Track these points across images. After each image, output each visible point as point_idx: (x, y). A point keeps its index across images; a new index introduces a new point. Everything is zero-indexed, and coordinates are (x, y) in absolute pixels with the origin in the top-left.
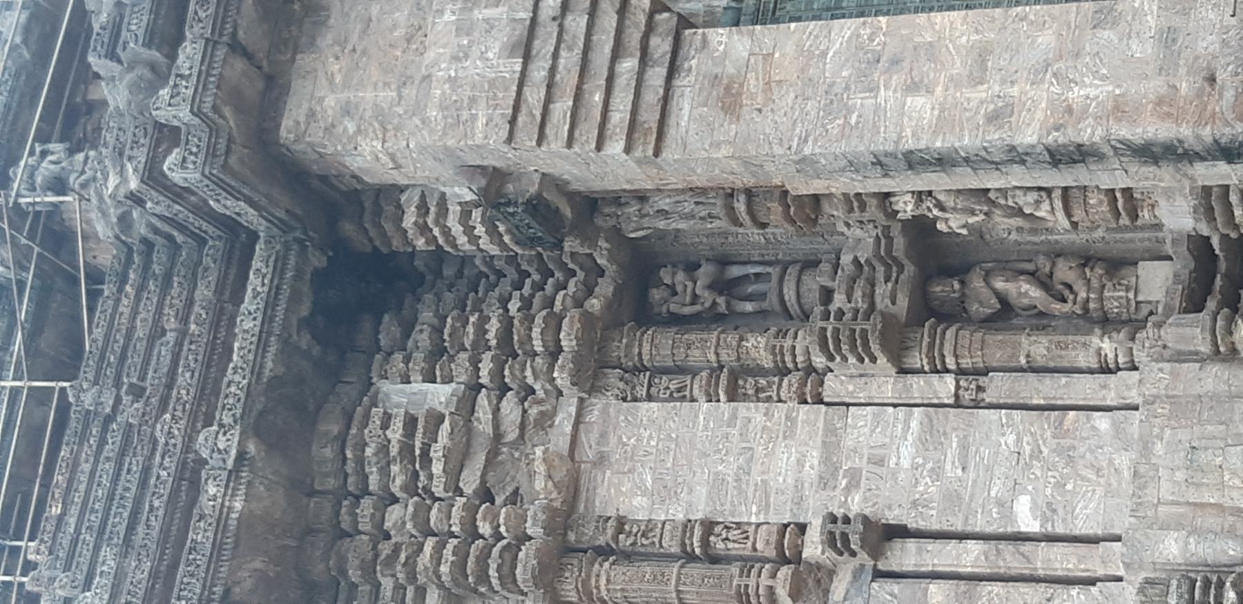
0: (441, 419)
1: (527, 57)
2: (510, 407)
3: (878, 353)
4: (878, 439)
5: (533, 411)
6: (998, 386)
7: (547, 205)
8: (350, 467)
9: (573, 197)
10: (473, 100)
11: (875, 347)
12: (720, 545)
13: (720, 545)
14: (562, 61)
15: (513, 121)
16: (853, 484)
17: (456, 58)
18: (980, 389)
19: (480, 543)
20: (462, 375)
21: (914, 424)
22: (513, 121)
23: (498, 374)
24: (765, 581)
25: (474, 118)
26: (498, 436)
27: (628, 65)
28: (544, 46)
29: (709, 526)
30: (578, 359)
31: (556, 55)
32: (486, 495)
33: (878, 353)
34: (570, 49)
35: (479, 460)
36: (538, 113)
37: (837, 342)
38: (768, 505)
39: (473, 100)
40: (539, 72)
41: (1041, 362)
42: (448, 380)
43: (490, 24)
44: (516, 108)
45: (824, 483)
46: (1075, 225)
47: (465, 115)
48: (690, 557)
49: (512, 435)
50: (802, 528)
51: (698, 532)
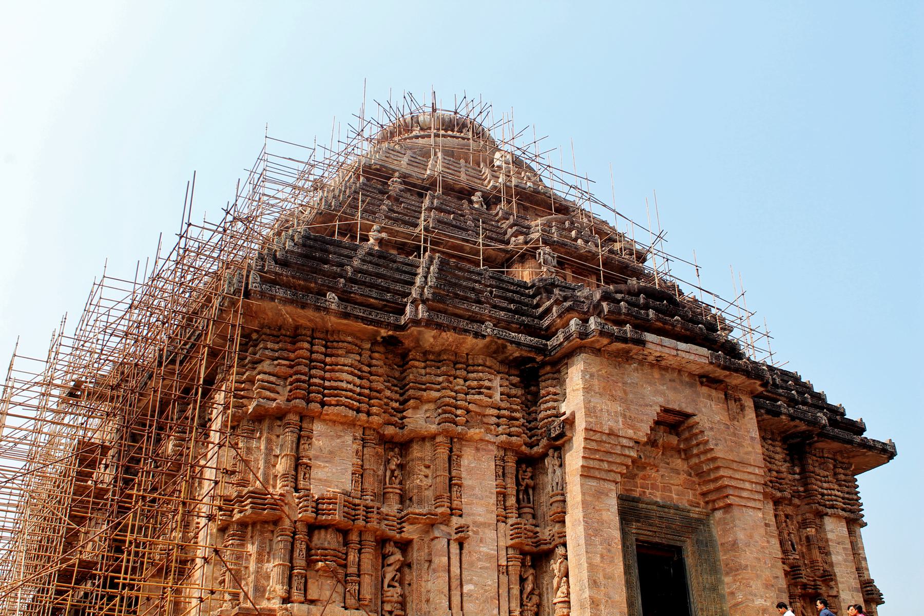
0: (490, 397)
1: (609, 434)
2: (494, 420)
3: (514, 541)
4: (488, 540)
5: (492, 427)
6: (504, 578)
7: (562, 438)
8: (476, 368)
9: (563, 445)
10: (597, 417)
11: (517, 540)
12: (455, 489)
13: (455, 489)
18: (503, 573)
20: (503, 405)
21: (492, 552)
23: (503, 416)
24: (446, 504)
26: (484, 416)
27: (605, 466)
28: (612, 440)
29: (460, 486)
30: (510, 443)
31: (609, 443)
33: (514, 541)
34: (611, 448)
37: (518, 528)
38: (466, 504)
39: (597, 417)
40: (604, 438)
41: (511, 592)
44: (594, 431)
45: (474, 523)
46: (555, 604)
48: (451, 479)
49: (485, 420)
50: (461, 516)
51: (459, 482)
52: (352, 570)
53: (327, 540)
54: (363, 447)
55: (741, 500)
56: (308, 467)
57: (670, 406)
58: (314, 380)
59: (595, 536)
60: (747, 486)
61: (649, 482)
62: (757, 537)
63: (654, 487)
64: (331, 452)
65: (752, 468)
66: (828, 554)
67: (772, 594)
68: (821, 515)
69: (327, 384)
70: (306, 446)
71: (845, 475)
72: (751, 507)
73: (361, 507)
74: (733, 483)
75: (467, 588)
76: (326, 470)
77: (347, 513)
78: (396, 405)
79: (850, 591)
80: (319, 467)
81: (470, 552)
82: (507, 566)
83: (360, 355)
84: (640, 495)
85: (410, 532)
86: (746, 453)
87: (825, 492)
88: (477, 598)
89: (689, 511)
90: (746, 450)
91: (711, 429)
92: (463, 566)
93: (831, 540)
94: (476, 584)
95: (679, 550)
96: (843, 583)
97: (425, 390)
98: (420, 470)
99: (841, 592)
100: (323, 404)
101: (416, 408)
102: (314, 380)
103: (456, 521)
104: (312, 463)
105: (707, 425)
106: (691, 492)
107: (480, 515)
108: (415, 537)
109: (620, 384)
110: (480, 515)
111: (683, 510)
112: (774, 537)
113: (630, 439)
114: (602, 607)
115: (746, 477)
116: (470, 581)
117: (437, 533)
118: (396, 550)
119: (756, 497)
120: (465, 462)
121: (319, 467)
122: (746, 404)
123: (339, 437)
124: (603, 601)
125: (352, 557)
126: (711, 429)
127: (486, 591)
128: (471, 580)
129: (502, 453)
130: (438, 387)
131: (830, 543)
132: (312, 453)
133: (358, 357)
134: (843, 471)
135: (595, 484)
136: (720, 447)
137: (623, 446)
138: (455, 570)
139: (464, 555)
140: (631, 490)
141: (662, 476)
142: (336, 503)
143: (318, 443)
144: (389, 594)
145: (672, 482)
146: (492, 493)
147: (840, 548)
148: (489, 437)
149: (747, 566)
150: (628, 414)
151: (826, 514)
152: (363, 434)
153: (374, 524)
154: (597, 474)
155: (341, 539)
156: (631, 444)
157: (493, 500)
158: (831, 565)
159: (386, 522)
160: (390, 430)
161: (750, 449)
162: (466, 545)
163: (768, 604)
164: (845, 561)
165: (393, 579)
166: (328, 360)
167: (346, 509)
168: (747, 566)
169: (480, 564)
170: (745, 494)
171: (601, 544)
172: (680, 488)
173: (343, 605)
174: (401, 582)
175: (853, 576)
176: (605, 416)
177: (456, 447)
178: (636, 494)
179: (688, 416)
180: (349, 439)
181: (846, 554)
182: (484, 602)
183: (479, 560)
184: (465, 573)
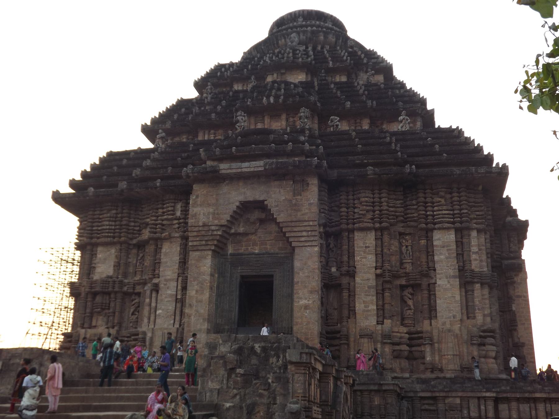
2: (177, 226)
10: (196, 218)
14: (203, 232)
15: (192, 226)
16: (165, 285)
17: (204, 213)
19: (155, 226)
22: (192, 226)
25: (193, 219)
27: (204, 242)
28: (206, 228)
29: (159, 263)
32: (163, 225)
35: (168, 223)
36: (194, 230)
40: (200, 229)
42: (181, 214)
43: (209, 218)
44: (194, 226)
45: (166, 280)
47: (194, 218)
50: (159, 277)
52: (111, 310)
53: (98, 299)
54: (121, 253)
55: (301, 243)
56: (94, 268)
57: (248, 200)
58: (94, 228)
59: (194, 281)
60: (304, 234)
61: (251, 242)
62: (310, 263)
63: (255, 244)
64: (105, 259)
65: (308, 222)
66: (433, 255)
67: (314, 296)
68: (432, 230)
69: (99, 228)
70: (94, 259)
71: (460, 197)
72: (309, 246)
73: (111, 283)
74: (292, 234)
75: (159, 312)
76: (102, 267)
77: (103, 286)
78: (138, 228)
79: (447, 278)
80: (99, 267)
81: (161, 295)
82: (182, 298)
83: (117, 210)
84: (244, 251)
85: (138, 289)
86: (303, 215)
87: (435, 213)
88: (163, 317)
89: (277, 254)
90: (303, 212)
91: (277, 206)
92: (158, 302)
93: (437, 246)
94: (163, 310)
95: (272, 276)
96: (442, 273)
97: (144, 219)
98: (147, 258)
99: (437, 280)
100: (98, 238)
101: (145, 228)
102: (94, 228)
103: (155, 281)
104: (96, 266)
105: (273, 205)
106: (281, 242)
107: (169, 275)
108: (141, 291)
109: (214, 196)
110: (169, 275)
111: (272, 254)
112: (371, 254)
113: (217, 225)
114: (192, 317)
115: (303, 229)
116: (160, 309)
117: (146, 288)
118: (137, 297)
119: (312, 239)
120: (163, 250)
121: (99, 267)
122: (310, 183)
123: (109, 251)
124: (194, 314)
125: (112, 305)
126: (277, 206)
127: (168, 312)
128: (161, 308)
129: (184, 241)
130: (149, 216)
131: (435, 248)
132: (95, 262)
133: (114, 212)
134: (458, 194)
135: (197, 254)
136: (282, 215)
137: (213, 231)
138: (153, 304)
139: (158, 296)
140: (239, 249)
141: (260, 237)
142: (96, 283)
143: (99, 256)
144: (131, 318)
145: (267, 239)
146: (176, 263)
147: (444, 251)
148: (177, 235)
149: (298, 282)
150: (216, 212)
151: (435, 229)
152: (121, 247)
153: (116, 289)
154: (200, 248)
155: (108, 298)
156: (217, 228)
157: (177, 266)
158: (433, 261)
159: (128, 286)
160: (134, 241)
161: (307, 211)
162: (160, 292)
163: (310, 302)
164: (447, 258)
165: (135, 311)
166: (101, 217)
167: (102, 285)
168: (298, 282)
169: (166, 300)
170: (303, 239)
171: (197, 285)
172: (274, 241)
173: (106, 326)
174: (138, 312)
175: (453, 268)
176: (202, 216)
177: (159, 243)
178: (241, 251)
179: (263, 201)
180: (113, 251)
181: (449, 254)
182: (166, 318)
183: (166, 297)
184: (158, 305)
